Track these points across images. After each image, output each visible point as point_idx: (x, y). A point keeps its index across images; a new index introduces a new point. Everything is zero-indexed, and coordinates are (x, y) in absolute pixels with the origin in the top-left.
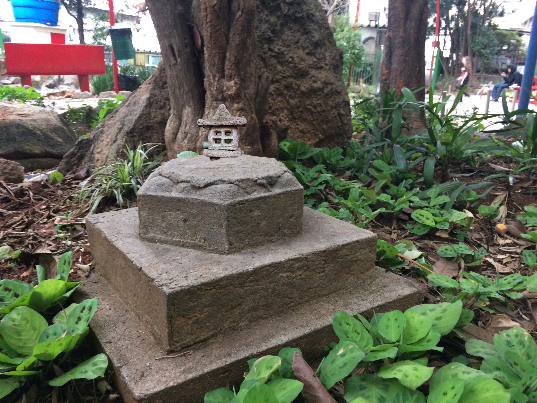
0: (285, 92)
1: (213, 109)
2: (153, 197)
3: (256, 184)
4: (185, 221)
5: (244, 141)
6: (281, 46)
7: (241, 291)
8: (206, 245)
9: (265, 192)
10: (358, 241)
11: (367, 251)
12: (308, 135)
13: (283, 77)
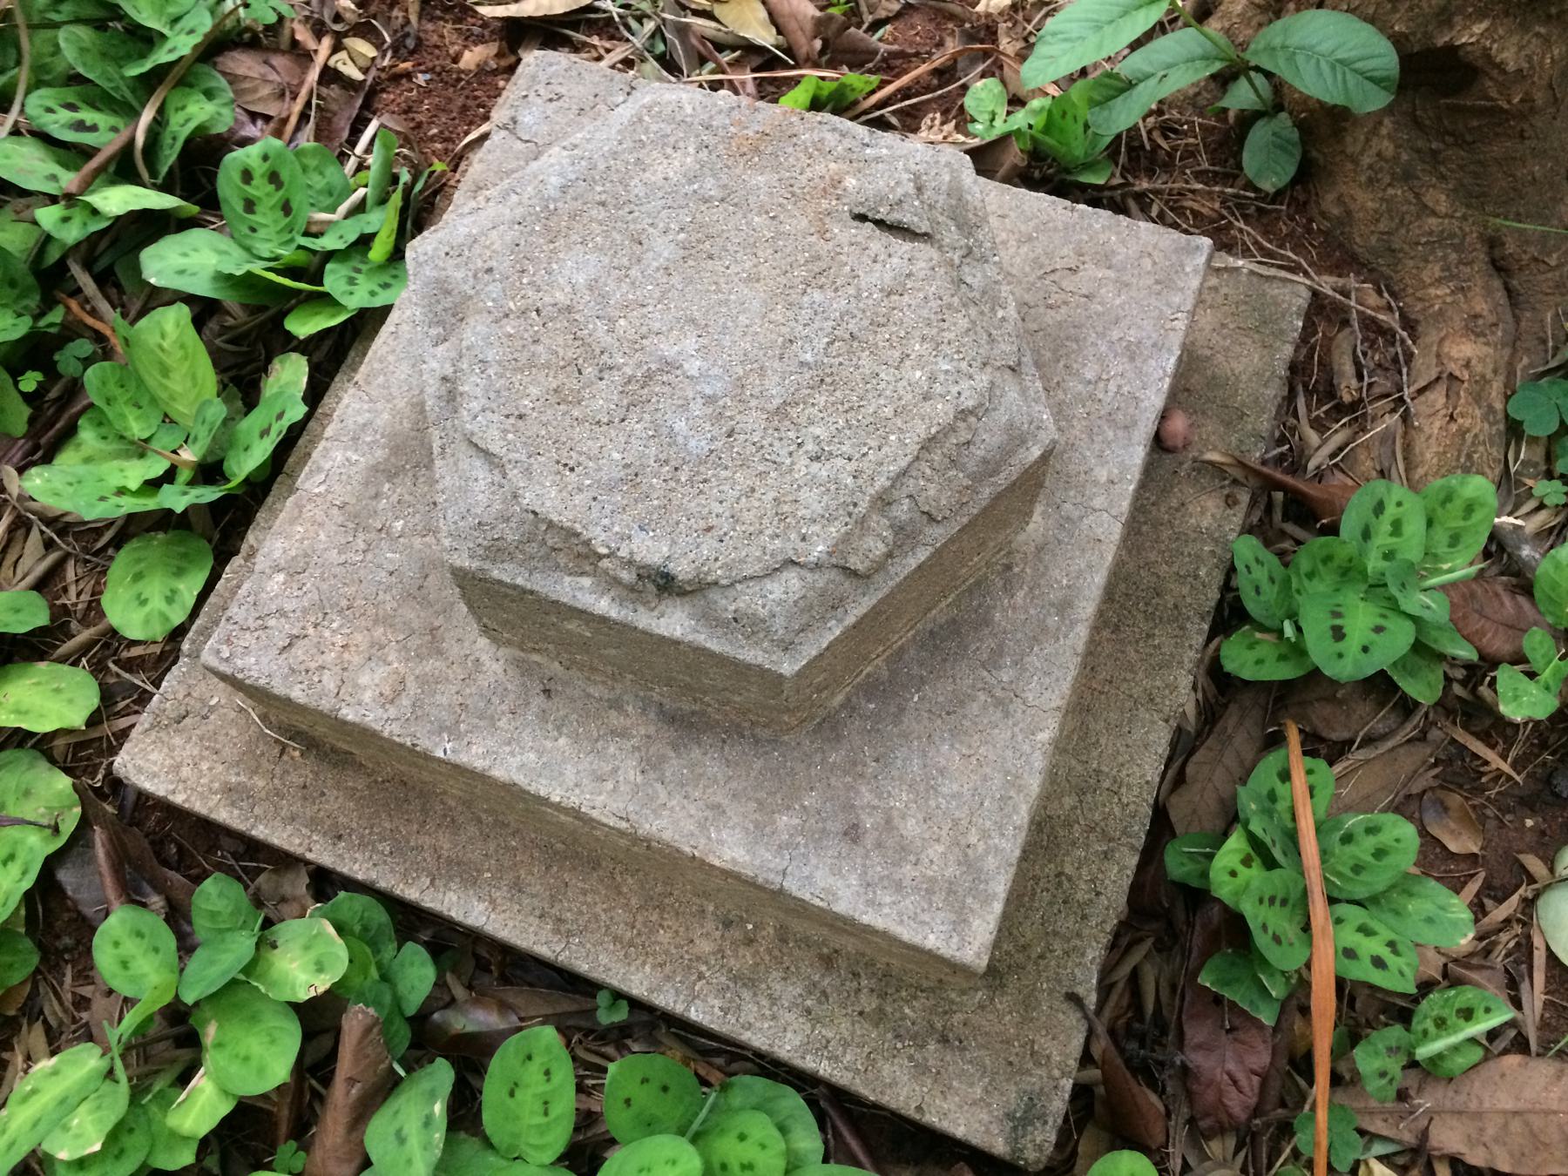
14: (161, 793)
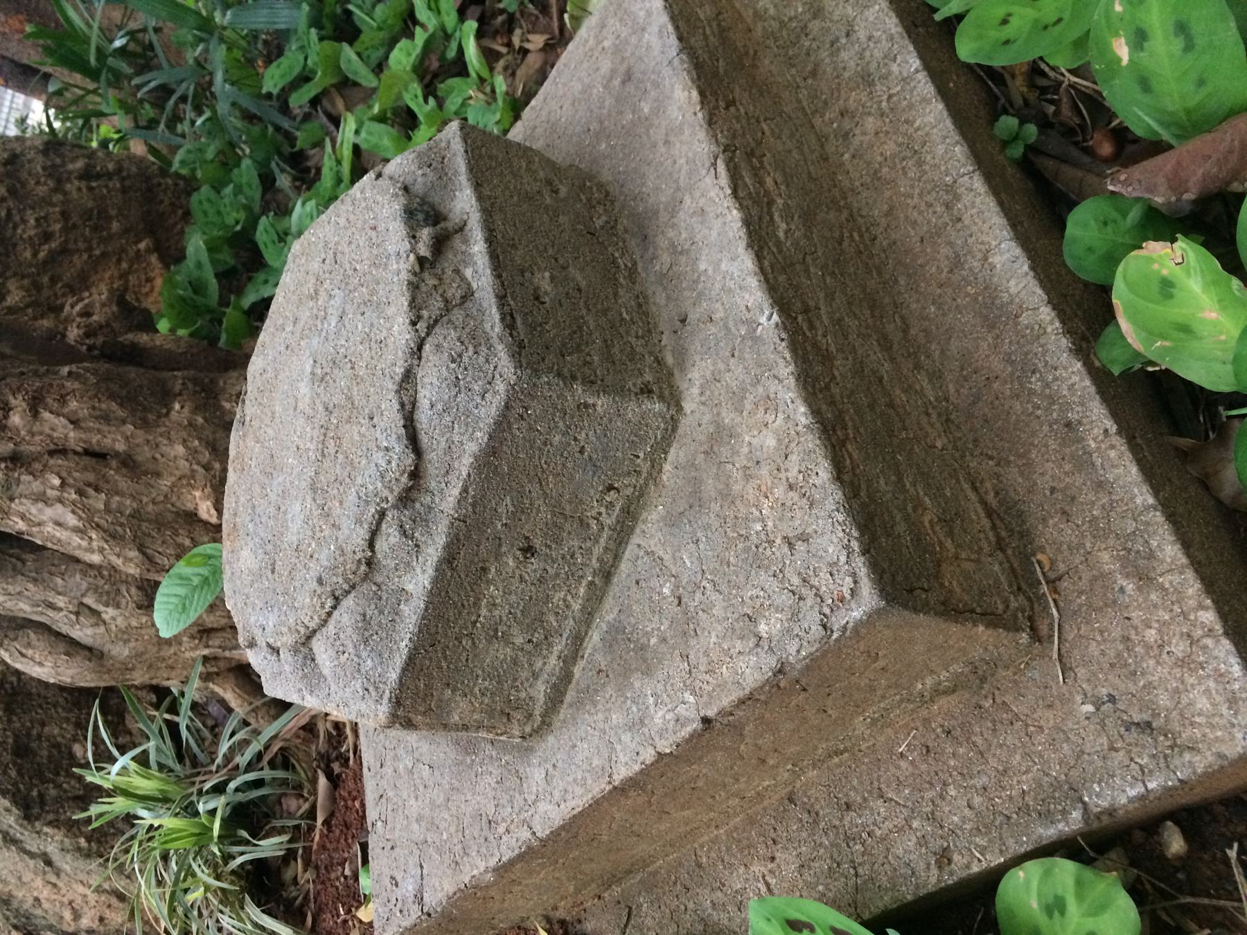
1: (12, 499)
2: (410, 663)
3: (433, 264)
4: (529, 551)
5: (151, 417)
8: (627, 484)
9: (466, 241)
12: (132, 279)
14: (1226, 644)
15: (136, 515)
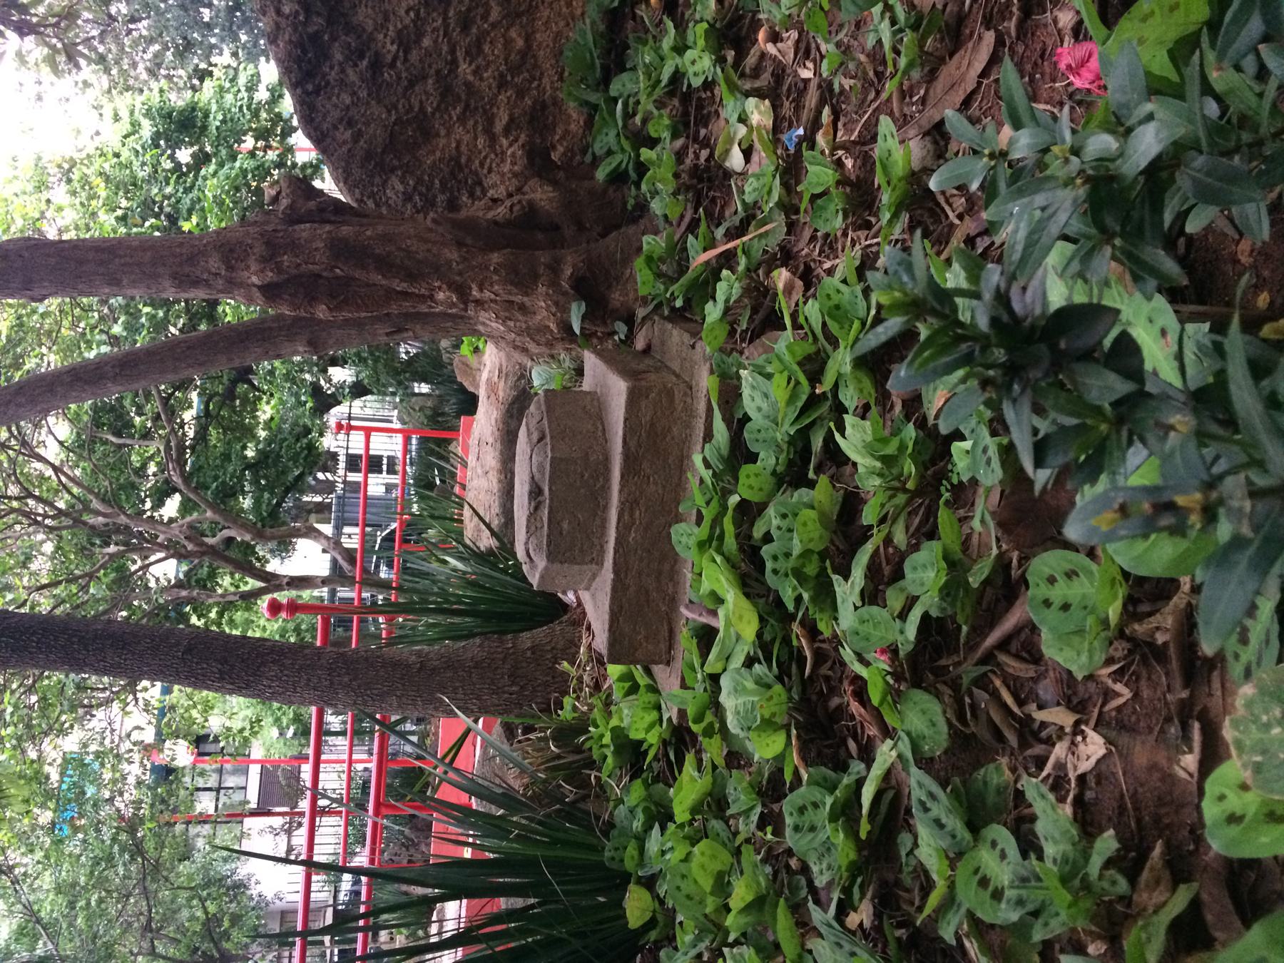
0: (474, 30)
6: (386, 36)
7: (632, 589)
10: (626, 420)
11: (643, 404)
13: (445, 36)
15: (528, 328)
